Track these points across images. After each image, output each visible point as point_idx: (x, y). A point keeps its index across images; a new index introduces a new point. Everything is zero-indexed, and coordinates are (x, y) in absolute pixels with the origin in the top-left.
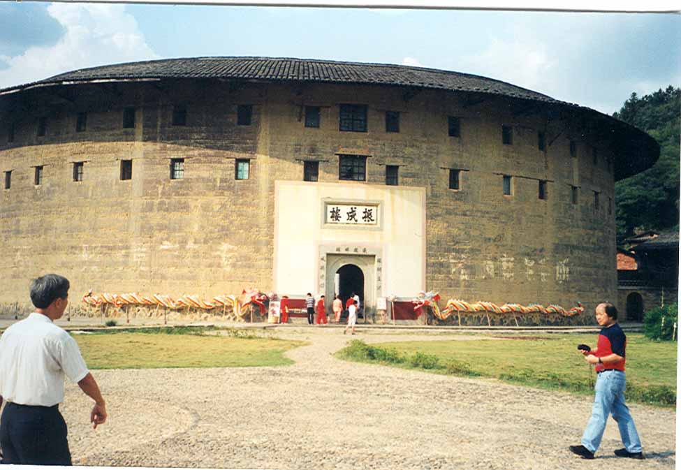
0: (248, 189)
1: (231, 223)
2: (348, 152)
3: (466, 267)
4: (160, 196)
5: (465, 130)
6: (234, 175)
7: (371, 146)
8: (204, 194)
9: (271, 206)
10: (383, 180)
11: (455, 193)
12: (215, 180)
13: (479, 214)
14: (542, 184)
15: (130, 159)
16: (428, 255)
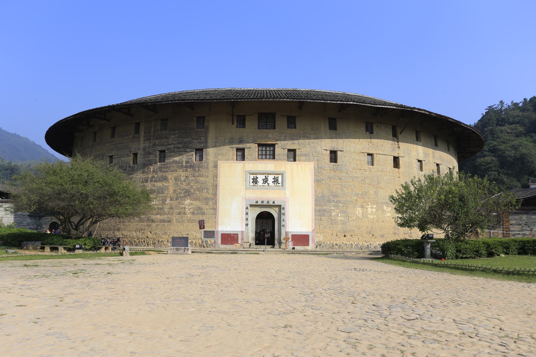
1: (192, 187)
3: (342, 212)
5: (339, 126)
7: (277, 138)
8: (176, 171)
9: (216, 176)
12: (182, 162)
16: (316, 205)
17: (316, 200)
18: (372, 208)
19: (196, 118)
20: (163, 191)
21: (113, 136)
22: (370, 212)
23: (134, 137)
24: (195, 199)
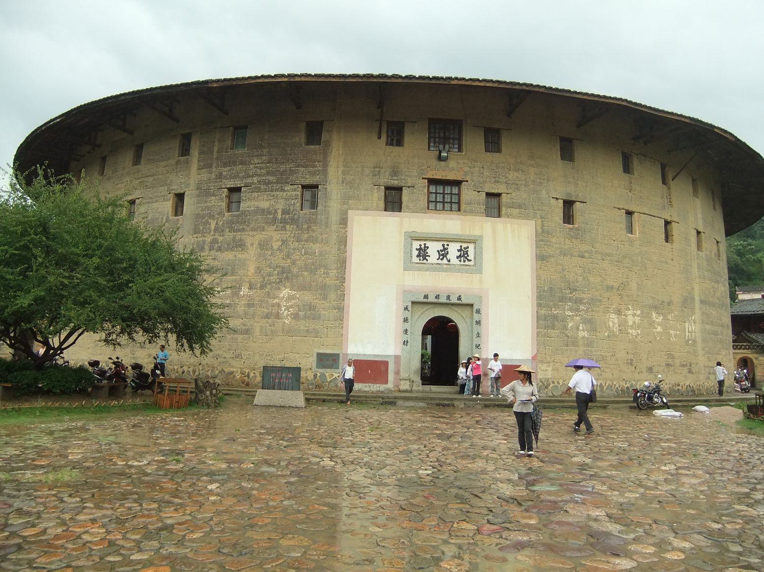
0: (315, 222)
2: (439, 176)
3: (587, 321)
4: (212, 233)
5: (580, 152)
6: (299, 205)
8: (263, 229)
9: (343, 242)
10: (483, 210)
11: (570, 228)
12: (276, 211)
13: (599, 257)
14: (667, 223)
15: (182, 192)
16: (539, 305)
17: (540, 297)
18: (634, 315)
19: (304, 124)
20: (233, 269)
21: (137, 161)
22: (630, 323)
23: (178, 162)
24: (302, 288)
